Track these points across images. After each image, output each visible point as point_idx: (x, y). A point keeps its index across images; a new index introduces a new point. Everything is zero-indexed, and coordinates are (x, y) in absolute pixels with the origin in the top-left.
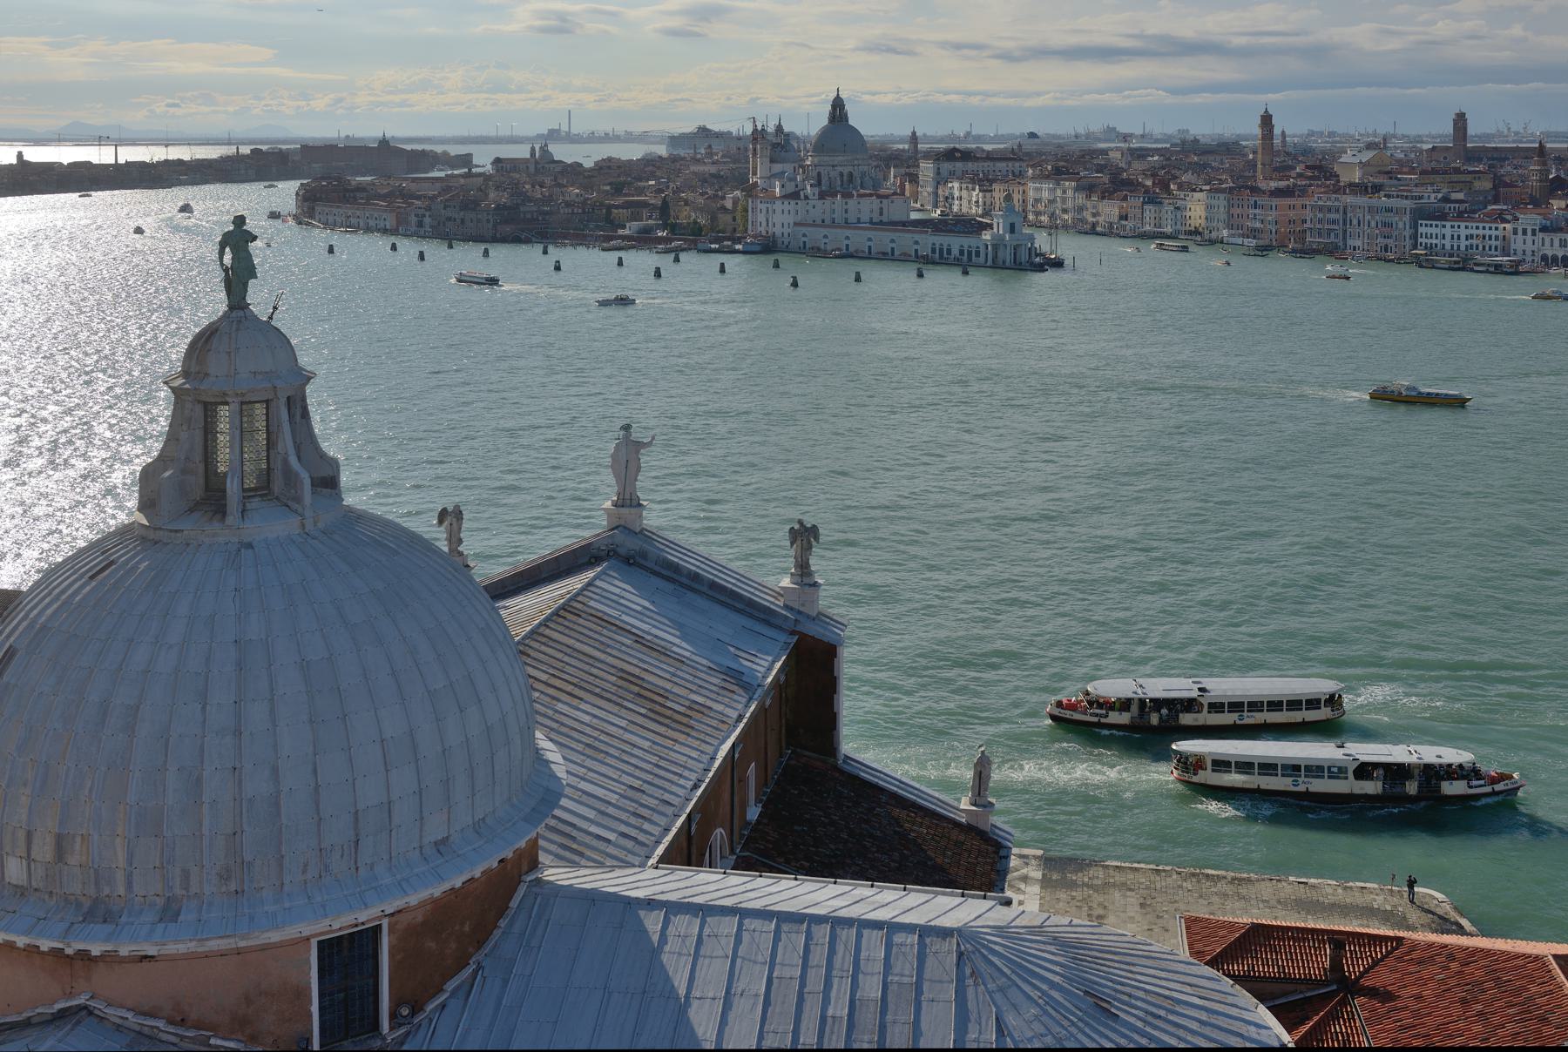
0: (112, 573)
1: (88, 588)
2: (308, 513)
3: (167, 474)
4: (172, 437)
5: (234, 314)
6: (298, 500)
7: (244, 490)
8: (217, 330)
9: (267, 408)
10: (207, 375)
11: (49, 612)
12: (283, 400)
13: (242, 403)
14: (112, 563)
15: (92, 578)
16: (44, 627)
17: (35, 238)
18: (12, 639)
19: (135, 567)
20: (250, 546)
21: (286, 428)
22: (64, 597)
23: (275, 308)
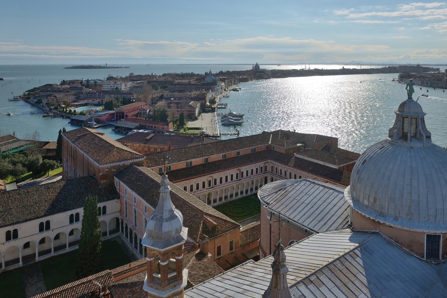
0: (384, 148)
1: (380, 151)
2: (425, 143)
3: (395, 131)
4: (396, 124)
5: (409, 100)
6: (423, 140)
7: (411, 136)
8: (406, 103)
9: (416, 120)
10: (404, 112)
11: (372, 154)
13: (411, 118)
14: (384, 147)
15: (380, 149)
16: (371, 157)
17: (373, 82)
18: (365, 158)
19: (389, 148)
20: (412, 148)
21: (420, 124)
22: (375, 152)
23: (418, 99)
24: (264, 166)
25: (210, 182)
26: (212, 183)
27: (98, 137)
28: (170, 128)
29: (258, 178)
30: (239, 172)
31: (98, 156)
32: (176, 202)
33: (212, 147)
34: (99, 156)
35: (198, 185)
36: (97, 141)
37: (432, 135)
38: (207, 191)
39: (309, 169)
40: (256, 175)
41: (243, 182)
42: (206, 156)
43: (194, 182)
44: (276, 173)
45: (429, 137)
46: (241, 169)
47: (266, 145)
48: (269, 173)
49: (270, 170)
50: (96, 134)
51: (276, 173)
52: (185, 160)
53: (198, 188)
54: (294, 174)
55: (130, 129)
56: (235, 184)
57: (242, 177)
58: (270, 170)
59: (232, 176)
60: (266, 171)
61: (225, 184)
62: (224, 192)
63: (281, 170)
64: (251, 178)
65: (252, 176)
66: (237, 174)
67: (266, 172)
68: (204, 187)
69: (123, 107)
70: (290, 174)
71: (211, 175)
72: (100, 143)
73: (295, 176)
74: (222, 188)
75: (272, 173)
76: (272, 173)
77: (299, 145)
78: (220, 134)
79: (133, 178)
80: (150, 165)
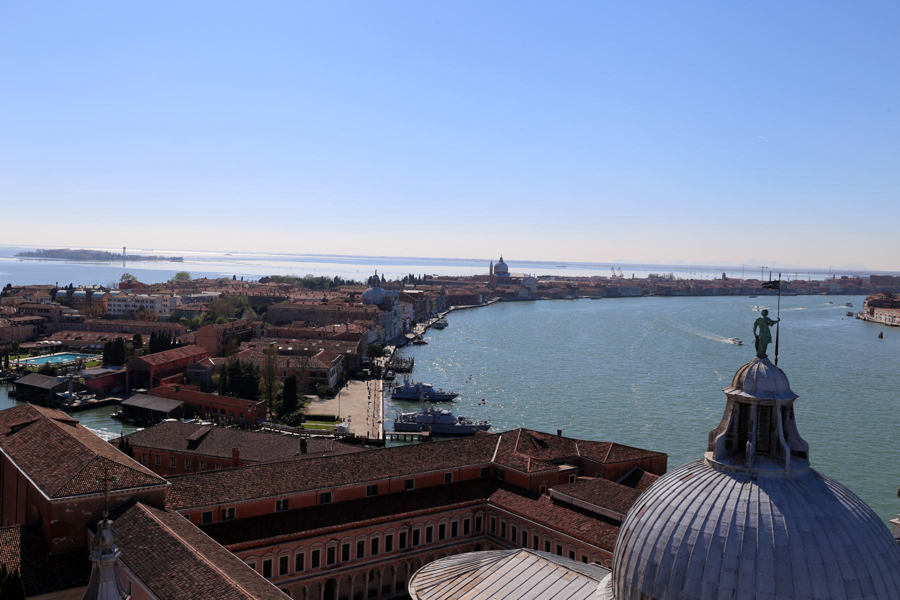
12: (779, 407)
24: (473, 517)
25: (331, 551)
26: (339, 556)
27: (58, 429)
28: (259, 416)
29: (456, 546)
30: (407, 531)
31: (50, 477)
32: (223, 596)
33: (343, 464)
34: (53, 476)
35: (300, 558)
36: (55, 438)
37: (810, 448)
38: (322, 575)
39: (582, 529)
40: (450, 540)
41: (418, 555)
42: (324, 487)
43: (289, 551)
44: (503, 535)
45: (801, 455)
46: (411, 523)
47: (481, 463)
48: (487, 536)
49: (488, 530)
50: (52, 420)
51: (503, 535)
52: (271, 495)
53: (300, 567)
54: (544, 539)
55: (159, 416)
56: (396, 560)
57: (416, 542)
58: (488, 530)
59: (389, 539)
60: (478, 529)
61: (370, 559)
62: (368, 580)
63: (514, 530)
64: (439, 546)
65: (442, 541)
66: (403, 536)
67: (478, 533)
68: (316, 563)
69: (147, 359)
70: (536, 539)
71: (335, 534)
72: (62, 443)
73: (548, 544)
74: (362, 568)
75: (494, 537)
76: (494, 537)
77: (564, 467)
78: (384, 435)
79: (131, 535)
80: (181, 503)
